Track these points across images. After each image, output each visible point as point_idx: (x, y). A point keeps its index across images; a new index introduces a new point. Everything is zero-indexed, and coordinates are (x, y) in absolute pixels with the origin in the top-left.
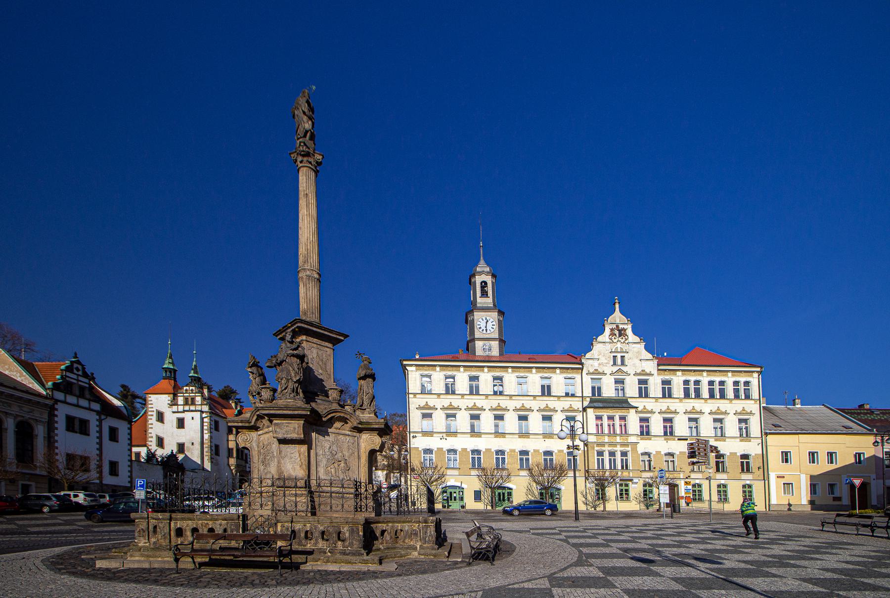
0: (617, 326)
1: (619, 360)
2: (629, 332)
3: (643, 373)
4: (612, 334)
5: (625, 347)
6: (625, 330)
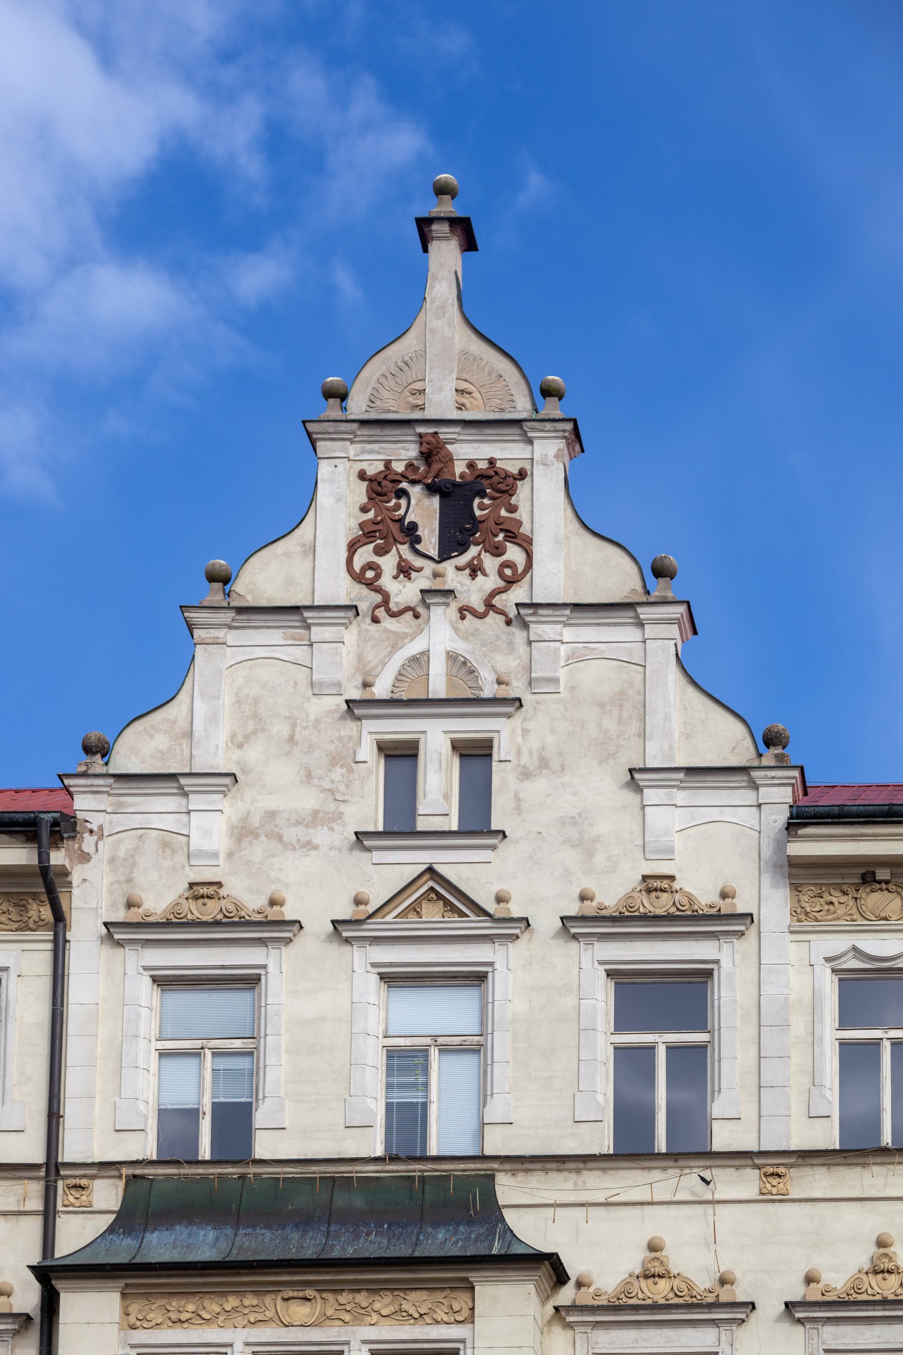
0: (433, 452)
1: (435, 779)
2: (543, 504)
3: (658, 909)
4: (383, 529)
5: (498, 657)
6: (499, 483)
